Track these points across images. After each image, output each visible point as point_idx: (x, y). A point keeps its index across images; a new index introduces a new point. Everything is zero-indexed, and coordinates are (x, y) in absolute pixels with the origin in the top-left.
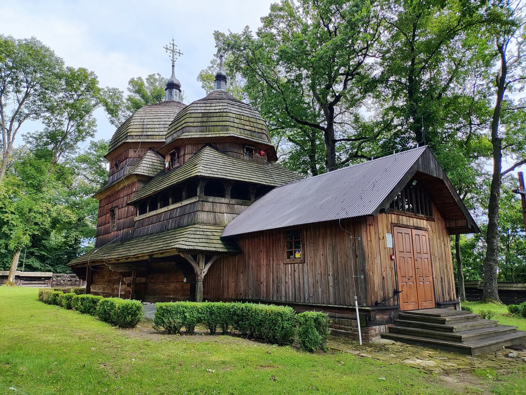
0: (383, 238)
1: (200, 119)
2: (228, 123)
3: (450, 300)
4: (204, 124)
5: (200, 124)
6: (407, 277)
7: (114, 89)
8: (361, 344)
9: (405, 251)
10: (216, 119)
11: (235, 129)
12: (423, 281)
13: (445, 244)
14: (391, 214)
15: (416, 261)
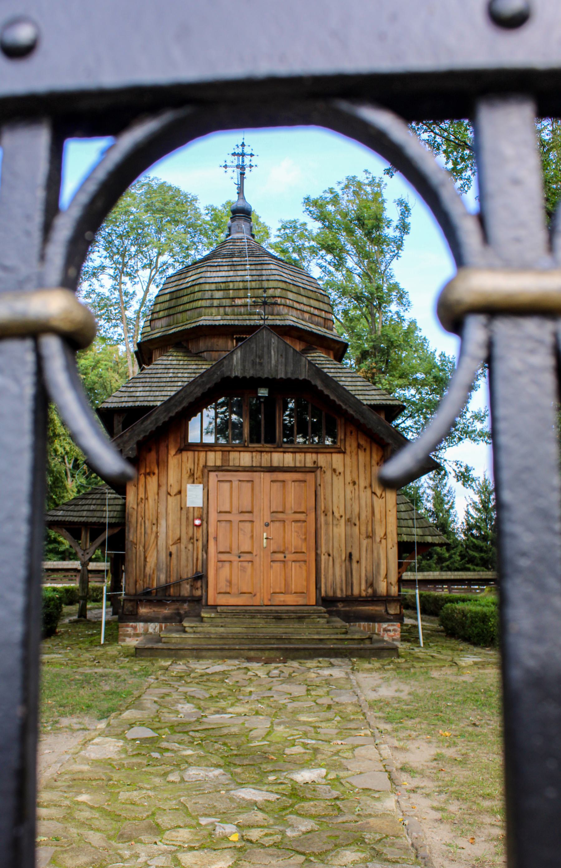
0: (180, 492)
1: (166, 305)
2: (200, 303)
3: (375, 592)
4: (172, 311)
5: (166, 313)
6: (235, 551)
7: (291, 222)
8: (102, 642)
9: (235, 511)
10: (185, 299)
11: (214, 310)
12: (283, 559)
13: (373, 493)
14: (206, 451)
15: (267, 525)
